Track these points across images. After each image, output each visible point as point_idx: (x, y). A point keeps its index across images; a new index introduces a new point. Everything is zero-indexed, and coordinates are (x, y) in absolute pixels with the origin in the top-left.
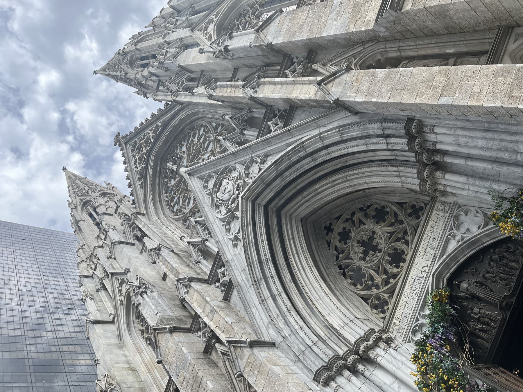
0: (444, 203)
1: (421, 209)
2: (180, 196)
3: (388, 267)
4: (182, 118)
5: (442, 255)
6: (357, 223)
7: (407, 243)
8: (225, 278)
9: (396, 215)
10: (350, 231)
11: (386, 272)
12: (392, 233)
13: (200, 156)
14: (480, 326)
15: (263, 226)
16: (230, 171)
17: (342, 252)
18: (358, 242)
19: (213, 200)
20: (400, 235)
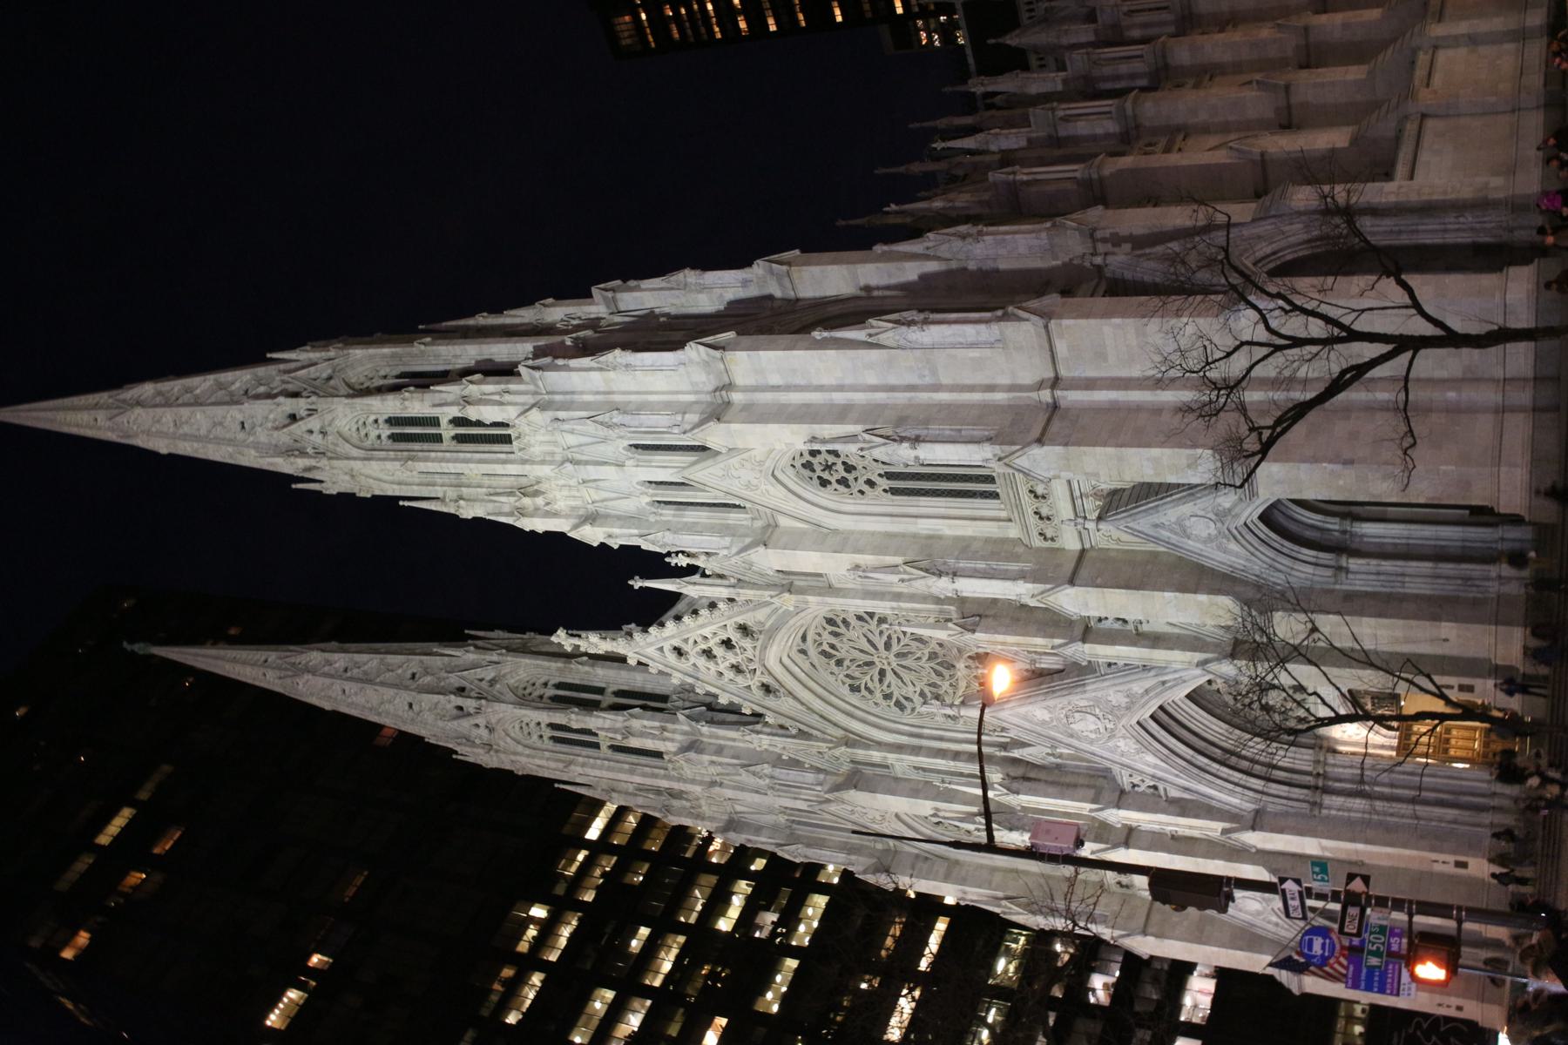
15: (1163, 733)
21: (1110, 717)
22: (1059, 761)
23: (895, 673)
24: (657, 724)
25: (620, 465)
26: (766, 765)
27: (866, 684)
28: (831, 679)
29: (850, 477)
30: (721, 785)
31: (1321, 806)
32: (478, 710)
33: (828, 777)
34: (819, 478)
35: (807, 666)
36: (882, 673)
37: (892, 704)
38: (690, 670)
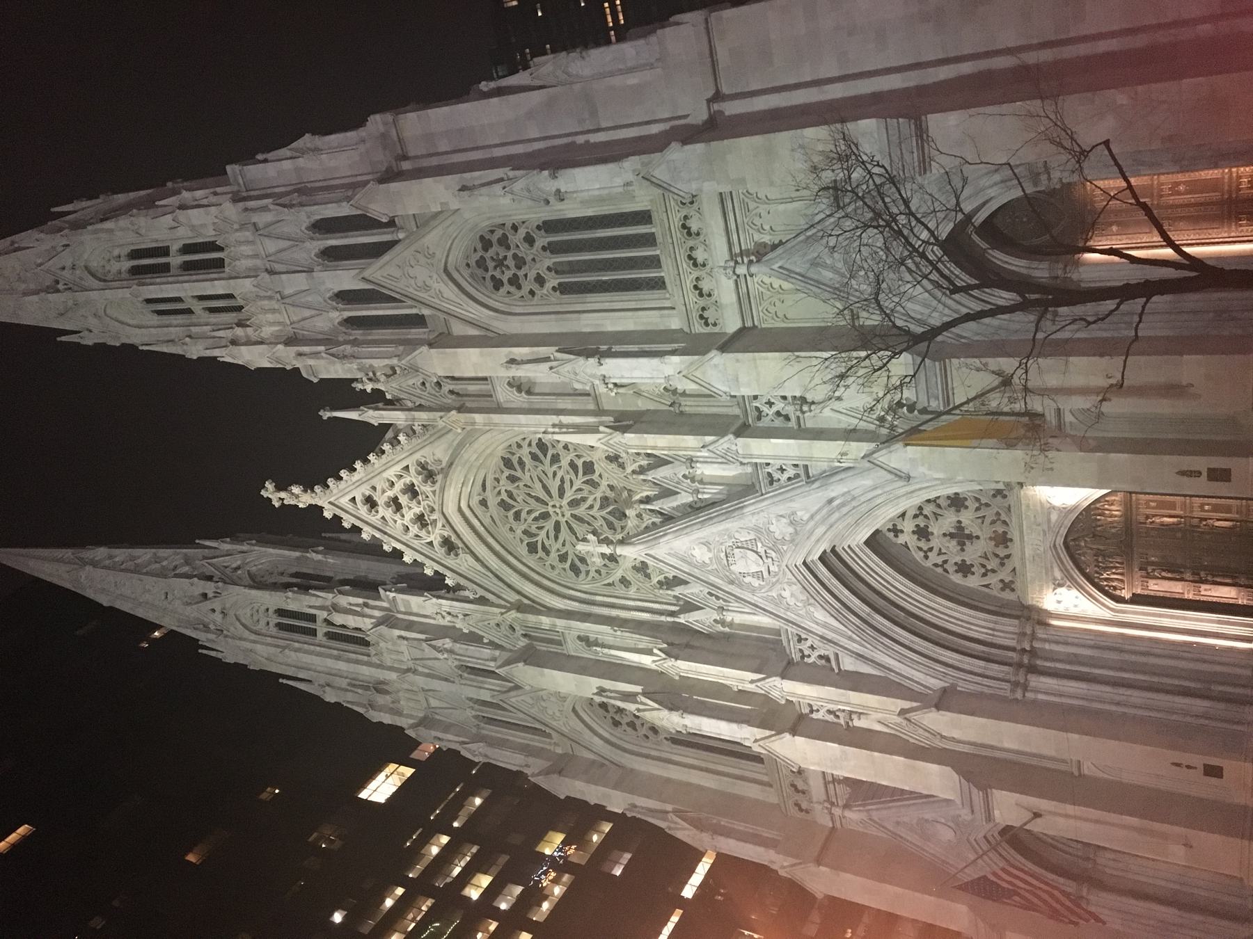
7: (1005, 522)
11: (997, 556)
12: (984, 517)
17: (931, 549)
21: (773, 555)
22: (727, 630)
23: (570, 528)
24: (360, 601)
25: (310, 271)
26: (447, 640)
27: (543, 543)
28: (510, 536)
29: (521, 273)
30: (415, 672)
31: (1025, 688)
32: (217, 594)
33: (504, 653)
34: (493, 277)
35: (487, 521)
36: (557, 526)
37: (567, 565)
38: (379, 524)
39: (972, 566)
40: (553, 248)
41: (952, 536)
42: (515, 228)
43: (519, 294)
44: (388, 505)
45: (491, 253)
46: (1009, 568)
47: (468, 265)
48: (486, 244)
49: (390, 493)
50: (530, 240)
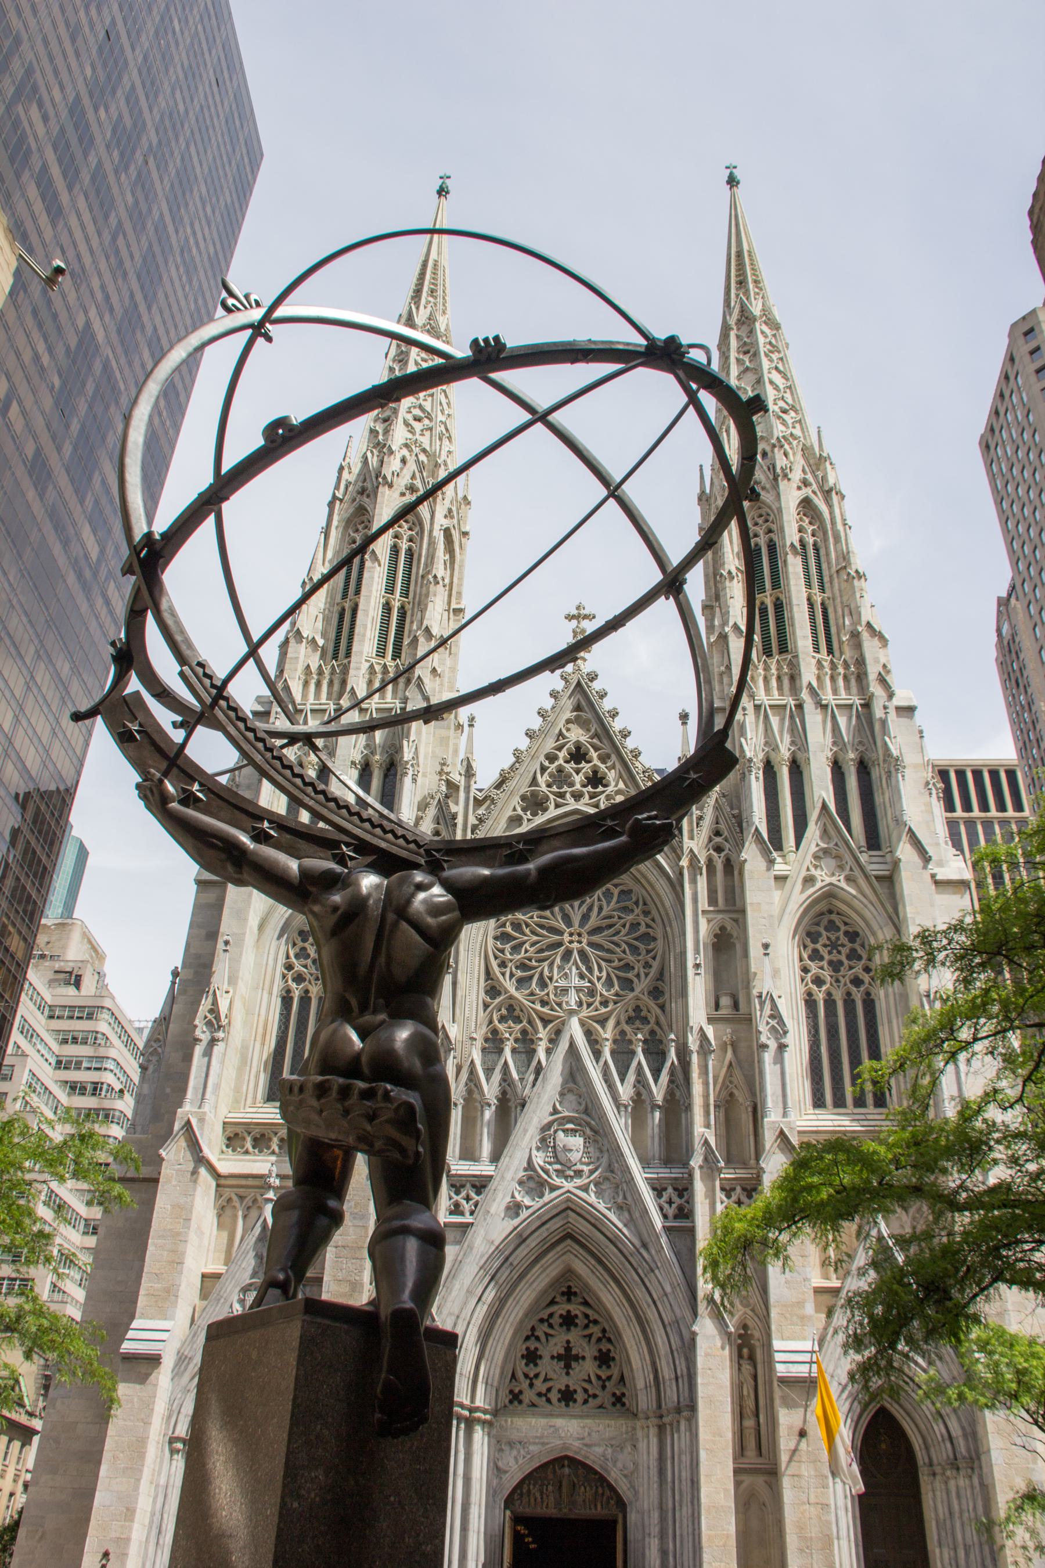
0: (634, 1429)
1: (623, 1405)
2: (527, 945)
3: (554, 1391)
4: (657, 886)
5: (586, 1445)
6: (587, 1332)
7: (586, 1402)
8: (464, 1202)
9: (609, 1378)
10: (576, 1325)
11: (549, 1390)
12: (589, 1381)
13: (603, 964)
14: (538, 1495)
16: (596, 1141)
17: (551, 1326)
18: (568, 1342)
19: (549, 1125)
20: (591, 1392)
29: (825, 963)
34: (820, 935)
39: (536, 1365)
40: (849, 1002)
41: (568, 1349)
42: (867, 970)
43: (805, 956)
44: (578, 746)
45: (844, 940)
46: (536, 1399)
47: (830, 912)
48: (853, 936)
49: (594, 755)
50: (857, 982)
